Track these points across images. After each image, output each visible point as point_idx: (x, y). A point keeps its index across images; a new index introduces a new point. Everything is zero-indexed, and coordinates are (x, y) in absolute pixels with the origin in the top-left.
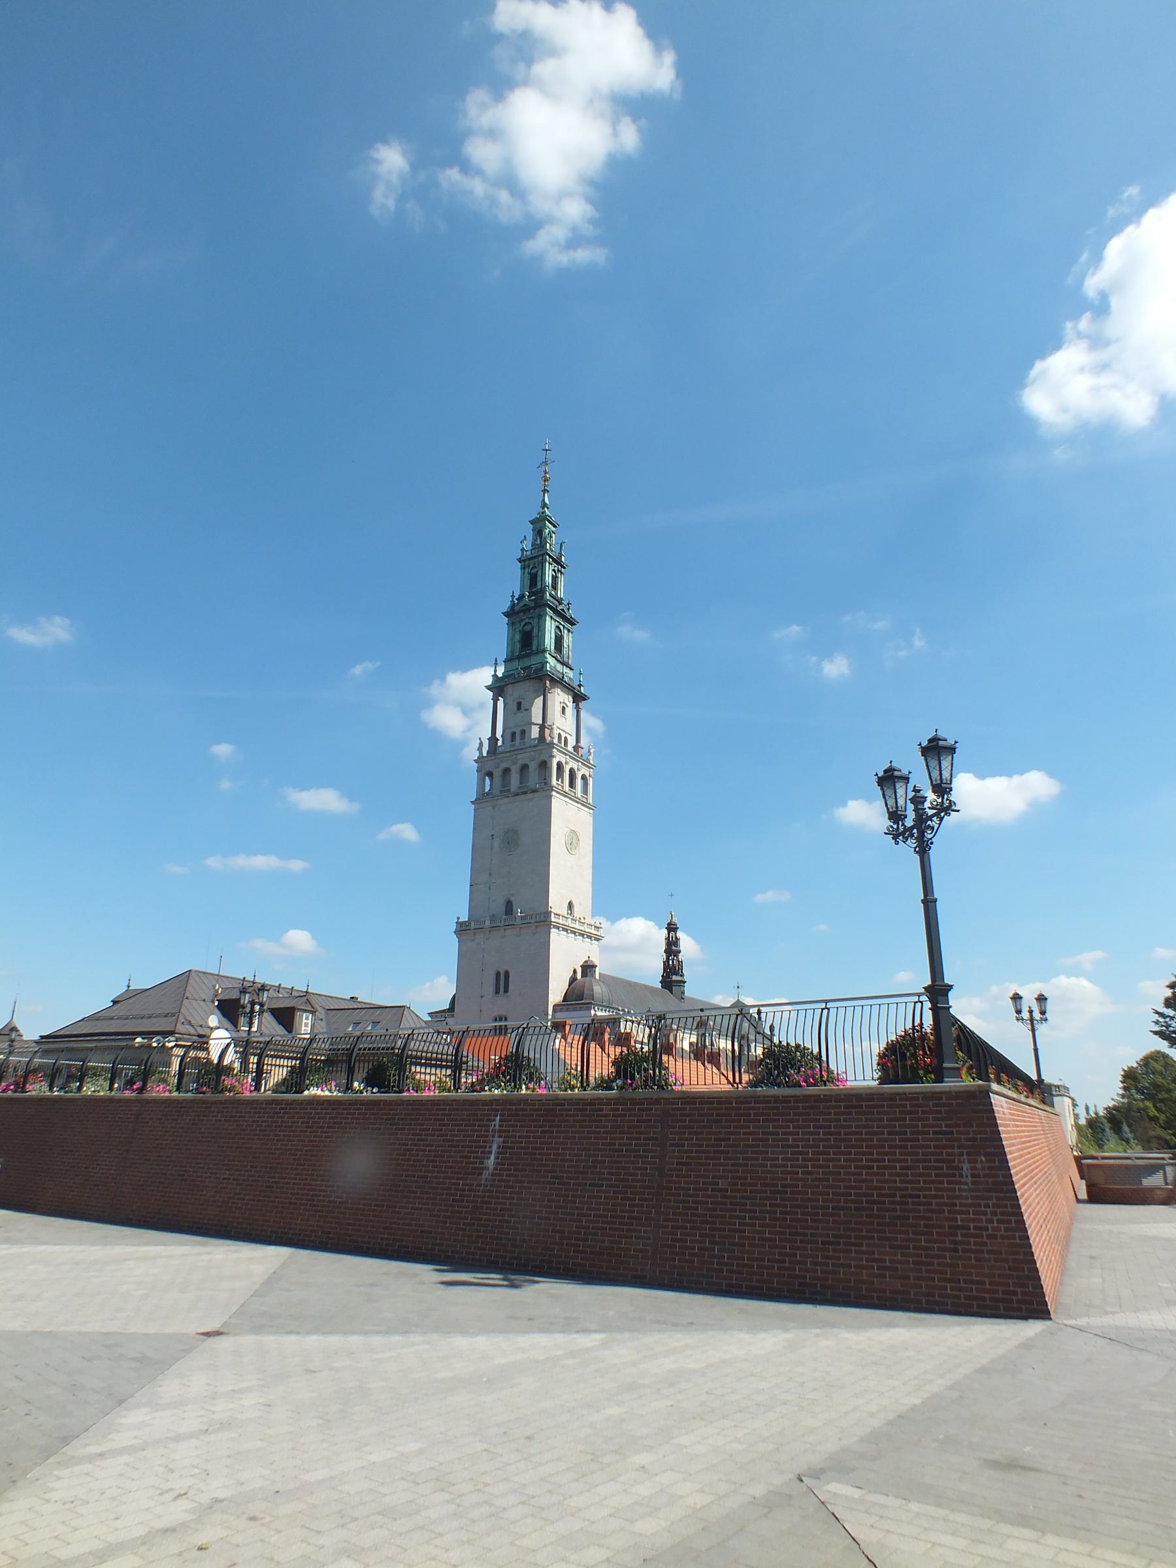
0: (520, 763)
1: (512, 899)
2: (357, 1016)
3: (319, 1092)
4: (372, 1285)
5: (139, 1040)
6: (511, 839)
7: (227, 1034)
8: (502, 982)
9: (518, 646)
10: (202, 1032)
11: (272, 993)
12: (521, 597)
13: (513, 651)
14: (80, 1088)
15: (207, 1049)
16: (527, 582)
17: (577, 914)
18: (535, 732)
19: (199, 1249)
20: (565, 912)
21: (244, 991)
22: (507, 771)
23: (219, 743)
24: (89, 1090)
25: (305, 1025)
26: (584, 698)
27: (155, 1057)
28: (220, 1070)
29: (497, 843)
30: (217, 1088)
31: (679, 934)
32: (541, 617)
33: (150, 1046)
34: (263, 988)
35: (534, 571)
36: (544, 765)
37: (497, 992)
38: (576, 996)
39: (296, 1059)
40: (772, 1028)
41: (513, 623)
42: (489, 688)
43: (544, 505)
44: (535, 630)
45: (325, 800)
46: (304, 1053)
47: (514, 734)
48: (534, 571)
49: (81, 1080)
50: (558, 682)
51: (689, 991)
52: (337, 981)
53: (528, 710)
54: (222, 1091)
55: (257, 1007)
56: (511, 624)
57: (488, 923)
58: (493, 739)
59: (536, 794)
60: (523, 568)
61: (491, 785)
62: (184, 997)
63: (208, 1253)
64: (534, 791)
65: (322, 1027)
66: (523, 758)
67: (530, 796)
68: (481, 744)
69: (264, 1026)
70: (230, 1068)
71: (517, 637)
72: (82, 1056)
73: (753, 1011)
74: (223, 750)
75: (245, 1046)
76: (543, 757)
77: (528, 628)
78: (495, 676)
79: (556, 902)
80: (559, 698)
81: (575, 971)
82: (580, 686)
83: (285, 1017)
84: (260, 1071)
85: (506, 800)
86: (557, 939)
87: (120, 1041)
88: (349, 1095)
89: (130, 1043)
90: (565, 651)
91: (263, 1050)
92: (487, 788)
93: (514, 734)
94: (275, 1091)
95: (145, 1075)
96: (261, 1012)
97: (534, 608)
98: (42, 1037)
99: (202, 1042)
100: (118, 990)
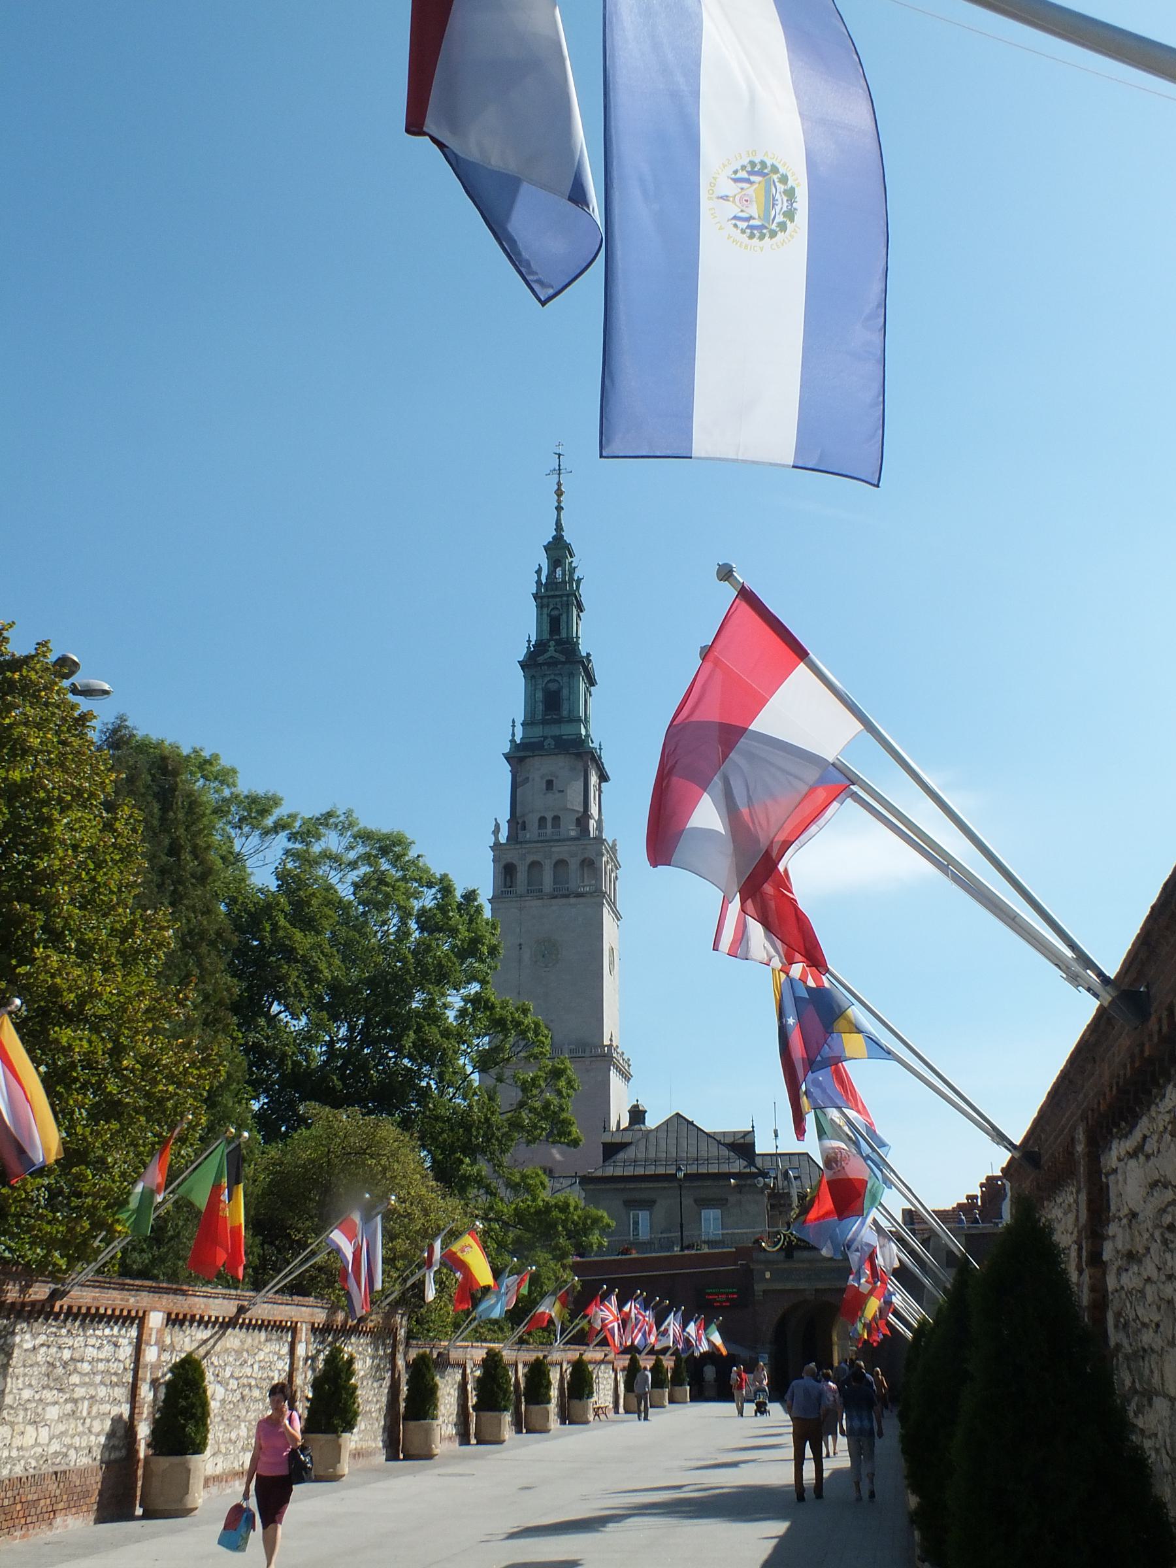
0: (555, 858)
6: (547, 951)
9: (540, 707)
16: (546, 627)
22: (535, 865)
29: (527, 955)
32: (572, 675)
42: (508, 757)
44: (565, 692)
48: (555, 613)
66: (560, 851)
67: (573, 900)
68: (497, 826)
71: (539, 695)
77: (553, 687)
78: (513, 741)
93: (542, 820)
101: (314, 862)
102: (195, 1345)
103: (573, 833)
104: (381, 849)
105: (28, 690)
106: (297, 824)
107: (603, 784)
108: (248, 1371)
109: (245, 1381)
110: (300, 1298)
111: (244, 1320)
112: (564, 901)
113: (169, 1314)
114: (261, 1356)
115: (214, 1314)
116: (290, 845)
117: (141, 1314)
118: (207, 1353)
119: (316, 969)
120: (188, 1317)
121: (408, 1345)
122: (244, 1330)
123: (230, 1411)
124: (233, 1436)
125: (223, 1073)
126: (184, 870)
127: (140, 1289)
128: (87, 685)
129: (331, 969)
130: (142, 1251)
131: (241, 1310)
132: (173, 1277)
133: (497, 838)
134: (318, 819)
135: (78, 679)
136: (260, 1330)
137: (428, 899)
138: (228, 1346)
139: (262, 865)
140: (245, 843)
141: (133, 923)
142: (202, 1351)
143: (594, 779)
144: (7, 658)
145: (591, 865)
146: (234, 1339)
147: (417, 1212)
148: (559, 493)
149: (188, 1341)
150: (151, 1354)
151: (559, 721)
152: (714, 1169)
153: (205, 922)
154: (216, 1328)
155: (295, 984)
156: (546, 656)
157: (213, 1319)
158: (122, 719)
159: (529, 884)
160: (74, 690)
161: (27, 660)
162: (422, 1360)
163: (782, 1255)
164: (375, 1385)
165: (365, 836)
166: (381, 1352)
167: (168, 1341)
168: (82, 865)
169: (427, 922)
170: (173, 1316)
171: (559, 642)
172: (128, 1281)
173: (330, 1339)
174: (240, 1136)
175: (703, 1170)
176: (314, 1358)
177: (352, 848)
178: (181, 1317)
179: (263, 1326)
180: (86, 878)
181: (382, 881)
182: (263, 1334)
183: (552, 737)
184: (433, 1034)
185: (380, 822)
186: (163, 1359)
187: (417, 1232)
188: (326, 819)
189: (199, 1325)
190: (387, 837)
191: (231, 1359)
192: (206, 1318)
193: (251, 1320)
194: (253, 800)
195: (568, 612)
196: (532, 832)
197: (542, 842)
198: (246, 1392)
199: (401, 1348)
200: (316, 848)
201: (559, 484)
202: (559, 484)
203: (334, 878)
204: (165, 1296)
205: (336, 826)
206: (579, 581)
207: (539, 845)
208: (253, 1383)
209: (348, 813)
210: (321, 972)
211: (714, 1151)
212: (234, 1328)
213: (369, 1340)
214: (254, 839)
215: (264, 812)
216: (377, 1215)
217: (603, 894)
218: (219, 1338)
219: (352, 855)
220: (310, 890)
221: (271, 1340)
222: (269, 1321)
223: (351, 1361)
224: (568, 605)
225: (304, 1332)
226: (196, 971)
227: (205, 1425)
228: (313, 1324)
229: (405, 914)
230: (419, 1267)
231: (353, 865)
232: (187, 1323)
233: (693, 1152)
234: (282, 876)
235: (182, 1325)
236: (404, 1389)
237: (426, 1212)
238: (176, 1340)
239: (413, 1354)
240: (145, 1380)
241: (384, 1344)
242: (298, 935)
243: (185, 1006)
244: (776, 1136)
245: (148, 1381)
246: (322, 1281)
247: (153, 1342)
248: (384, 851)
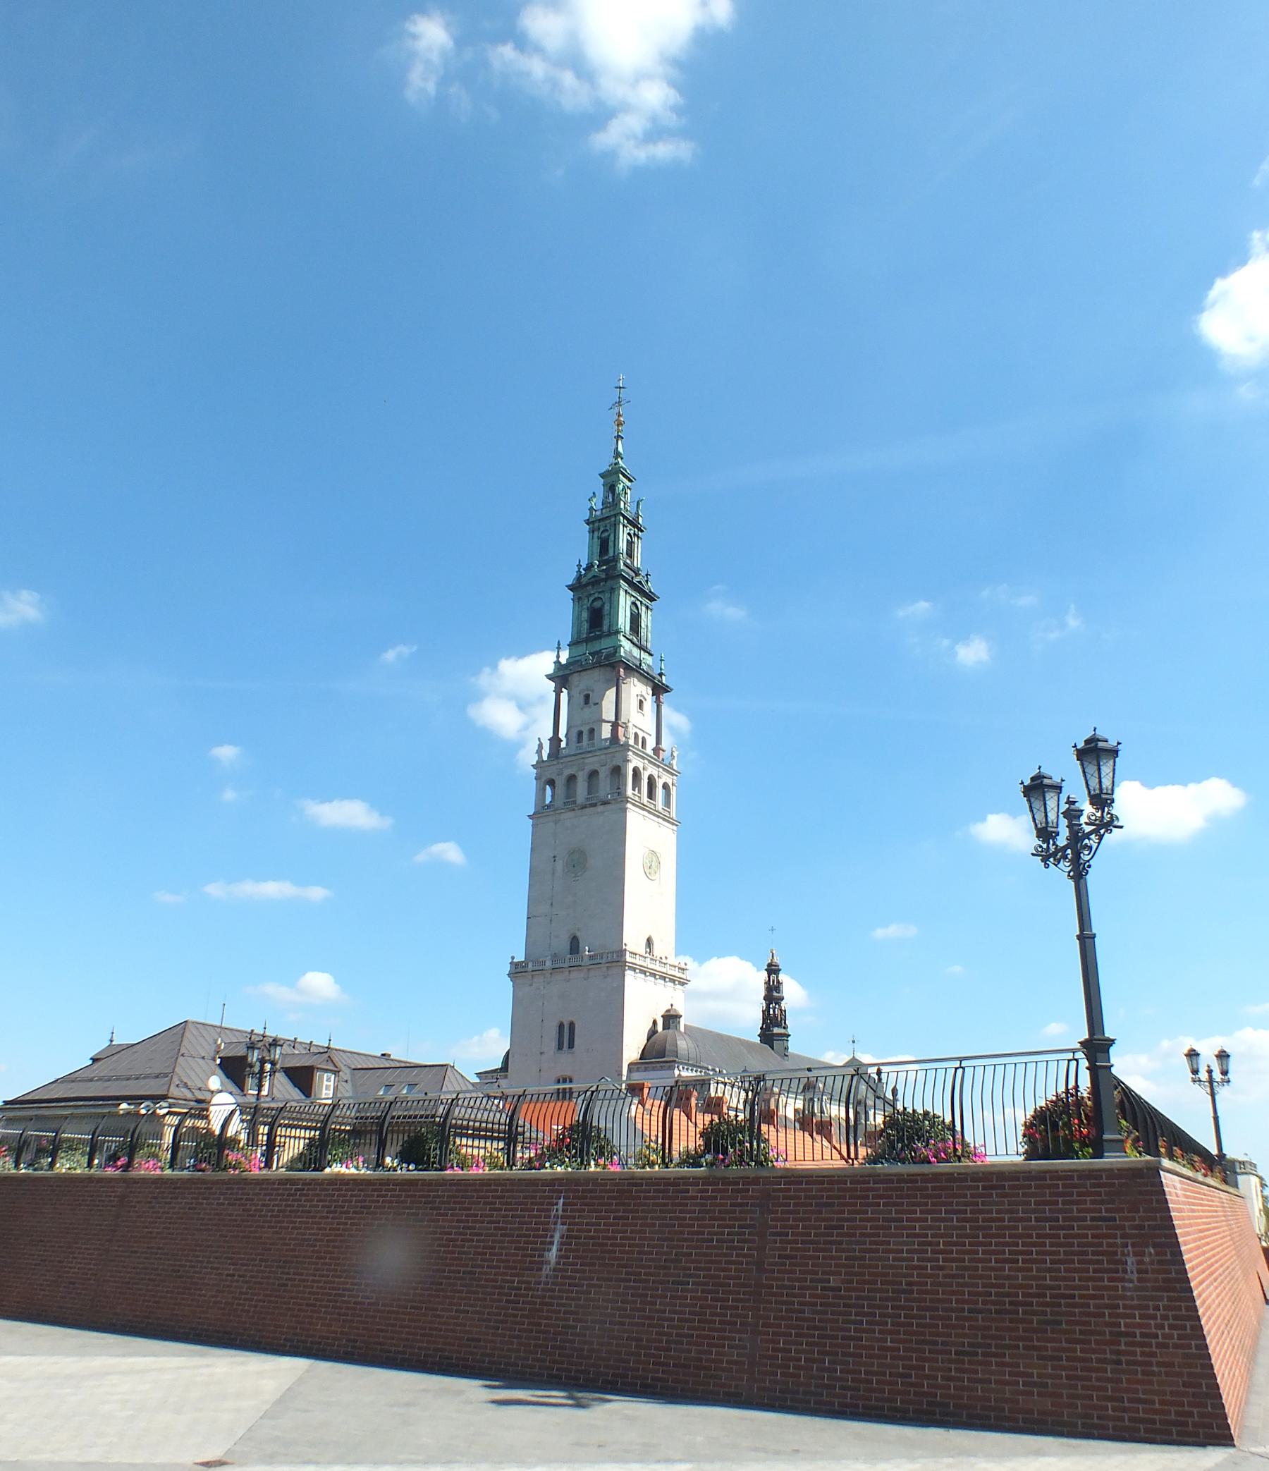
0: (588, 768)
1: (578, 934)
2: (389, 1077)
3: (343, 1170)
4: (407, 1405)
5: (124, 1106)
6: (577, 861)
7: (231, 1099)
8: (566, 1036)
9: (585, 626)
10: (200, 1097)
11: (287, 1049)
12: (590, 567)
13: (579, 632)
14: (52, 1165)
15: (207, 1117)
16: (597, 549)
17: (658, 950)
18: (606, 732)
19: (197, 1361)
20: (641, 949)
21: (251, 1047)
22: (572, 779)
23: (220, 744)
24: (63, 1166)
25: (326, 1087)
26: (666, 689)
27: (144, 1127)
28: (223, 1143)
29: (560, 865)
30: (220, 1165)
31: (782, 977)
32: (614, 591)
33: (137, 1114)
34: (275, 1043)
35: (606, 534)
36: (618, 772)
37: (560, 1047)
38: (657, 1052)
39: (315, 1129)
40: (894, 1092)
41: (580, 599)
42: (550, 677)
43: (618, 455)
44: (607, 607)
45: (349, 814)
46: (325, 1122)
47: (580, 734)
48: (606, 534)
49: (54, 1155)
50: (635, 670)
51: (794, 1046)
52: (362, 1037)
53: (598, 704)
54: (225, 1169)
55: (268, 1067)
56: (577, 600)
57: (548, 964)
58: (555, 740)
59: (608, 807)
60: (592, 531)
61: (553, 796)
62: (179, 1054)
63: (208, 1366)
64: (605, 803)
65: (347, 1091)
66: (592, 763)
67: (600, 808)
68: (540, 746)
69: (278, 1090)
70: (234, 1141)
71: (585, 615)
72: (54, 1125)
73: (872, 1071)
74: (226, 753)
75: (253, 1114)
76: (616, 762)
77: (597, 604)
78: (557, 662)
79: (633, 940)
80: (635, 689)
81: (655, 1022)
82: (661, 675)
83: (302, 1078)
84: (271, 1144)
85: (571, 814)
86: (633, 982)
87: (103, 1106)
88: (380, 1173)
89: (113, 1110)
90: (643, 632)
91: (275, 1118)
92: (548, 800)
93: (580, 734)
94: (289, 1169)
95: (132, 1150)
96: (273, 1072)
97: (606, 580)
98: (6, 1103)
99: (201, 1109)
100: (99, 1046)
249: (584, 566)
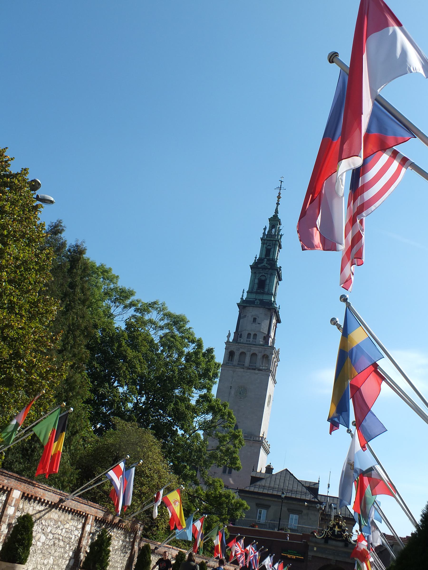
0: (252, 352)
6: (242, 392)
9: (256, 286)
16: (264, 253)
29: (233, 392)
32: (272, 275)
41: (255, 273)
42: (239, 305)
44: (268, 281)
48: (269, 247)
64: (259, 370)
66: (254, 349)
67: (257, 371)
68: (229, 334)
71: (257, 281)
77: (263, 278)
85: (242, 370)
93: (249, 335)
97: (269, 269)
101: (144, 323)
102: (35, 512)
103: (261, 343)
104: (174, 322)
105: (13, 187)
106: (140, 305)
107: (278, 324)
108: (59, 532)
109: (57, 536)
110: (92, 503)
111: (62, 506)
112: (253, 371)
113: (24, 493)
114: (67, 526)
115: (47, 499)
116: (135, 313)
117: (9, 489)
118: (40, 518)
119: (135, 367)
120: (34, 497)
121: (141, 540)
122: (61, 511)
123: (46, 549)
124: (46, 562)
125: (64, 376)
126: (76, 296)
127: (11, 477)
128: (44, 197)
129: (142, 369)
130: (20, 463)
131: (61, 501)
132: (31, 477)
133: (228, 339)
134: (149, 304)
135: (39, 192)
136: (69, 513)
137: (190, 348)
138: (52, 517)
139: (120, 318)
140: (116, 310)
141: (39, 300)
142: (38, 516)
143: (274, 321)
144: (7, 173)
145: (267, 358)
146: (55, 514)
147: (156, 476)
148: (279, 197)
149: (31, 508)
150: (10, 511)
151: (263, 293)
152: (298, 497)
153: (81, 321)
154: (47, 507)
155: (124, 372)
156: (262, 265)
157: (46, 501)
158: (60, 222)
159: (239, 362)
160: (38, 198)
161: (15, 176)
162: (147, 547)
163: (323, 541)
164: (122, 555)
165: (169, 315)
166: (128, 540)
167: (21, 506)
168: (18, 267)
169: (189, 357)
170: (26, 495)
171: (268, 260)
172: (5, 471)
173: (103, 527)
174: (69, 409)
175: (294, 496)
176: (94, 534)
177: (163, 320)
178: (30, 496)
179: (71, 511)
180: (19, 274)
181: (173, 336)
182: (70, 516)
183: (259, 300)
184: (182, 407)
185: (175, 310)
186: (17, 514)
187: (154, 486)
188: (153, 305)
189: (38, 503)
190: (178, 317)
191: (52, 524)
192: (42, 500)
193: (65, 507)
194: (123, 291)
195: (274, 248)
196: (244, 339)
197: (247, 344)
198: (57, 541)
199: (138, 540)
200: (147, 317)
201: (280, 194)
202: (280, 194)
203: (152, 332)
204: (24, 484)
205: (157, 309)
206: (281, 235)
207: (246, 345)
208: (61, 538)
209: (163, 304)
210: (137, 368)
211: (300, 488)
212: (56, 509)
213: (123, 532)
214: (120, 309)
215: (127, 297)
216: (133, 467)
217: (270, 371)
218: (48, 512)
219: (162, 323)
220: (139, 333)
221: (74, 519)
222: (74, 510)
223: (110, 539)
224: (275, 245)
225: (91, 520)
226: (72, 342)
227: (28, 550)
228: (96, 517)
229: (181, 354)
230: (152, 501)
231: (162, 328)
232: (32, 500)
233: (290, 487)
234: (129, 326)
235: (30, 500)
236: (136, 560)
237: (160, 477)
238: (25, 507)
239: (143, 544)
240: (5, 523)
241: (130, 536)
242: (129, 351)
243: (54, 343)
244: (329, 487)
245: (7, 523)
246: (103, 496)
247: (13, 505)
248: (175, 323)
249: (257, 258)
